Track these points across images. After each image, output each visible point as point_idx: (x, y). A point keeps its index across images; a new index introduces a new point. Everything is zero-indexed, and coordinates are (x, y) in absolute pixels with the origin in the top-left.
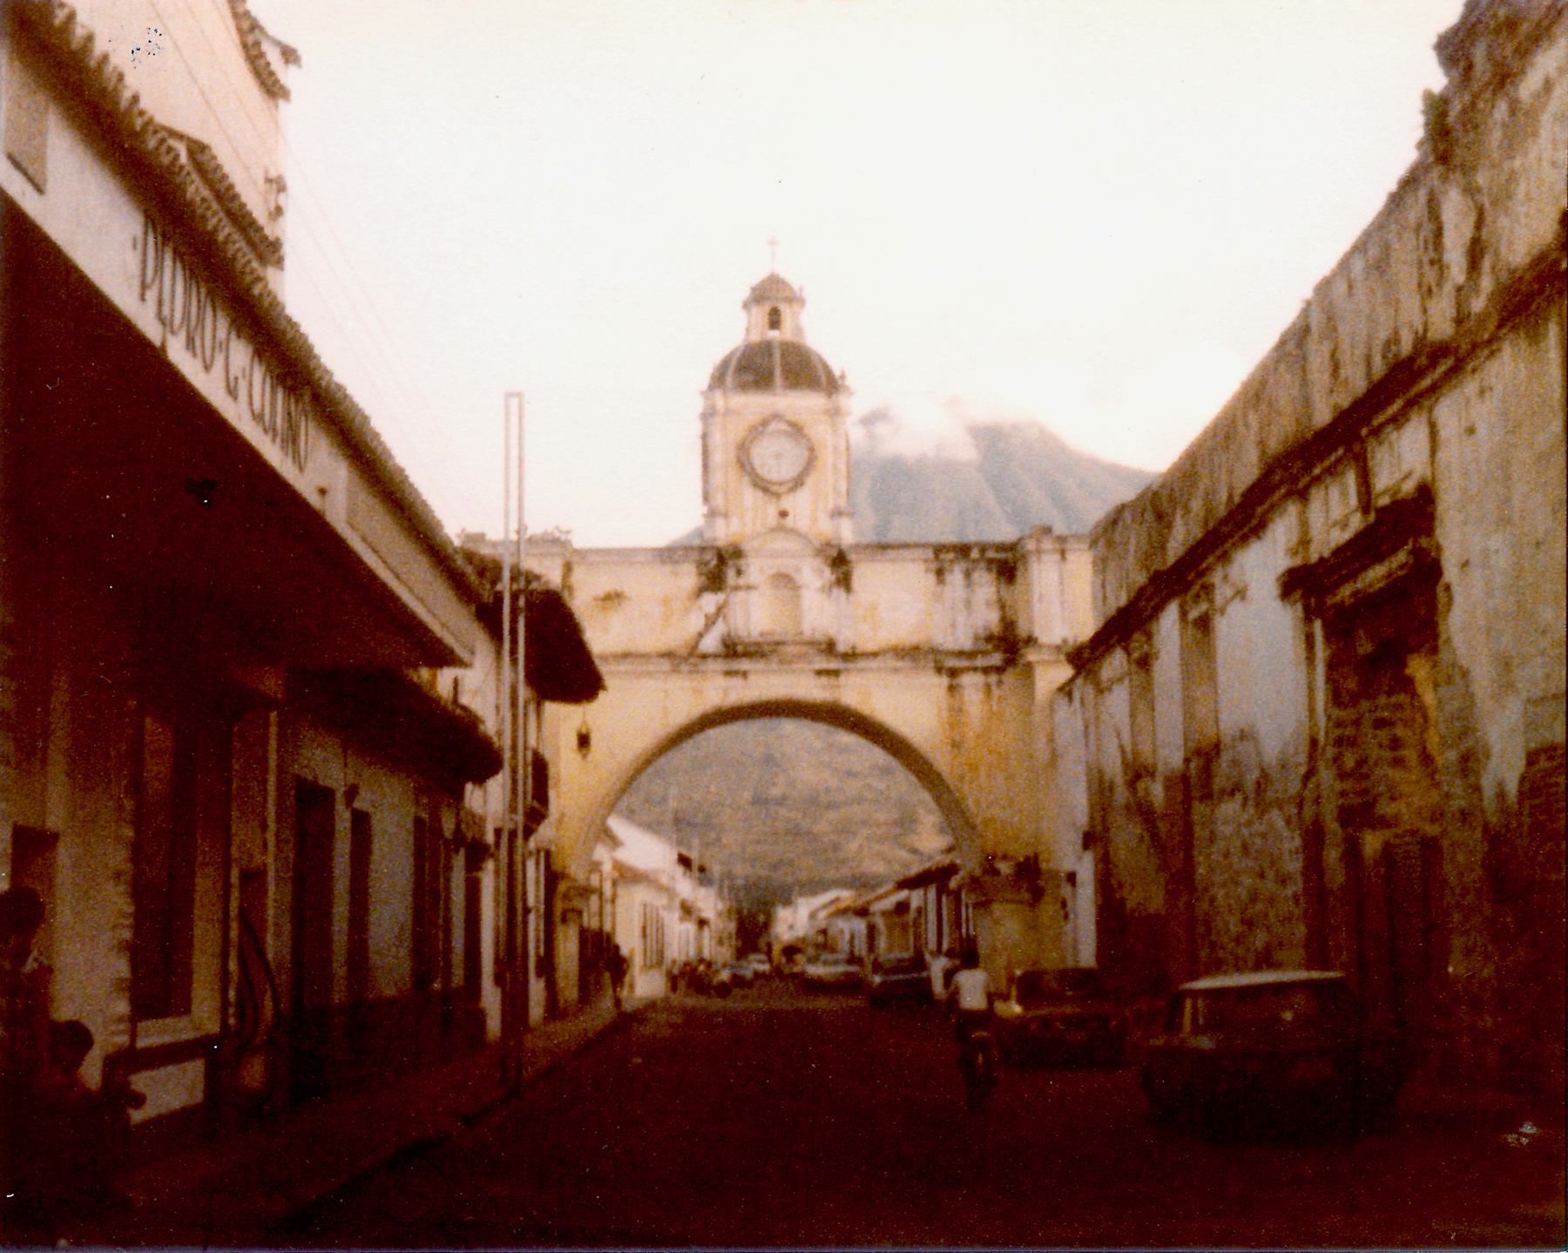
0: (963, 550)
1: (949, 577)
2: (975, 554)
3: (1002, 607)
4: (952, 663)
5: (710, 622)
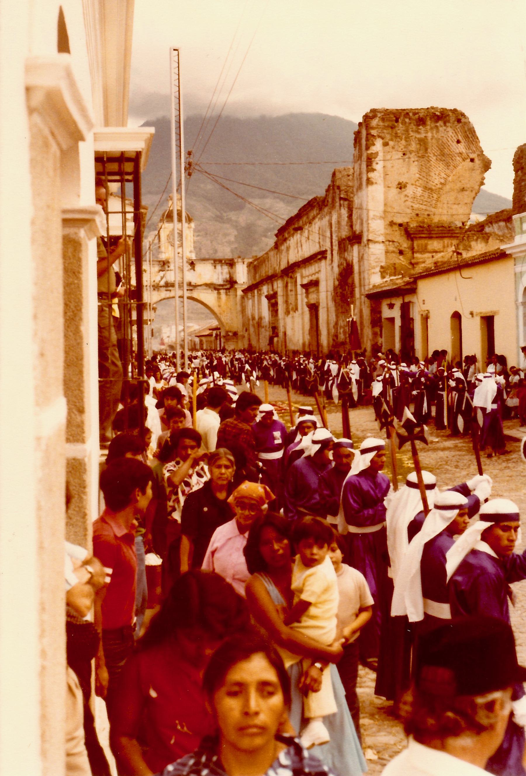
0: (220, 261)
1: (217, 267)
2: (223, 262)
3: (230, 273)
4: (218, 287)
5: (162, 278)
